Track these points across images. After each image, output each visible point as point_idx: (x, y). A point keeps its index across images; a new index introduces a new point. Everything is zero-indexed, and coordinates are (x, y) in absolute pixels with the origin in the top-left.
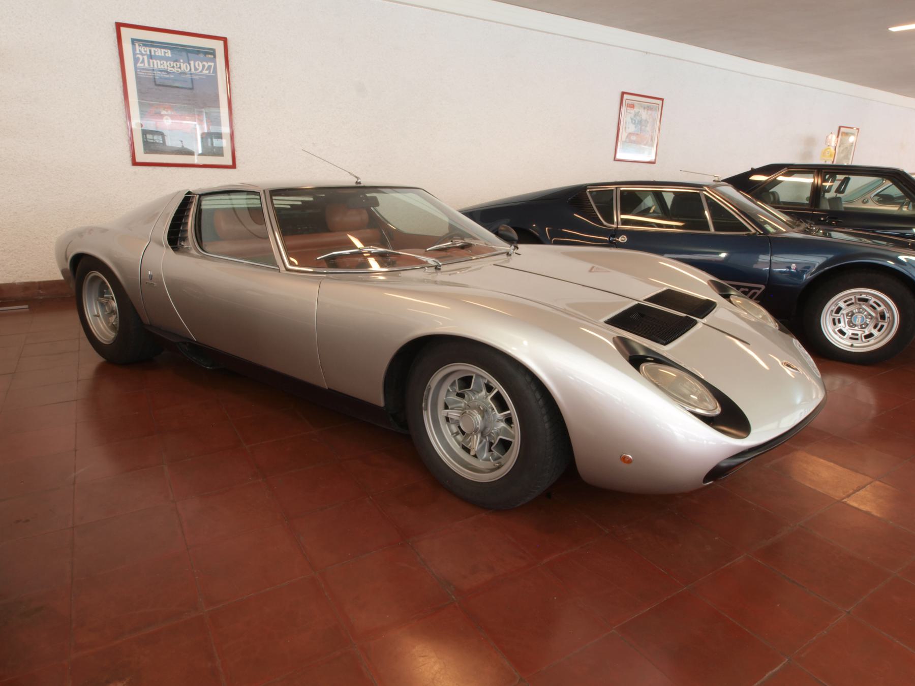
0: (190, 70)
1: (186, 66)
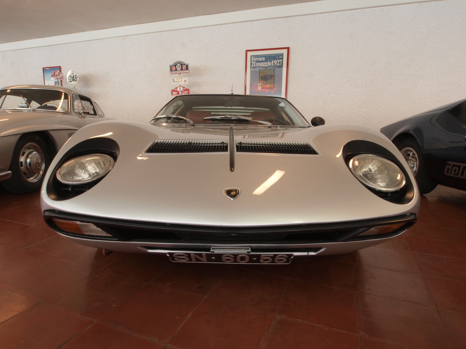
0: (272, 64)
1: (270, 63)
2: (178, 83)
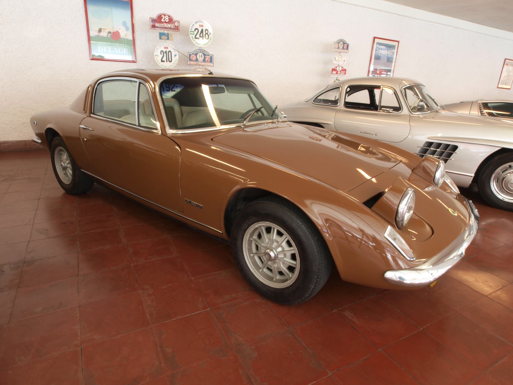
2: (338, 62)
